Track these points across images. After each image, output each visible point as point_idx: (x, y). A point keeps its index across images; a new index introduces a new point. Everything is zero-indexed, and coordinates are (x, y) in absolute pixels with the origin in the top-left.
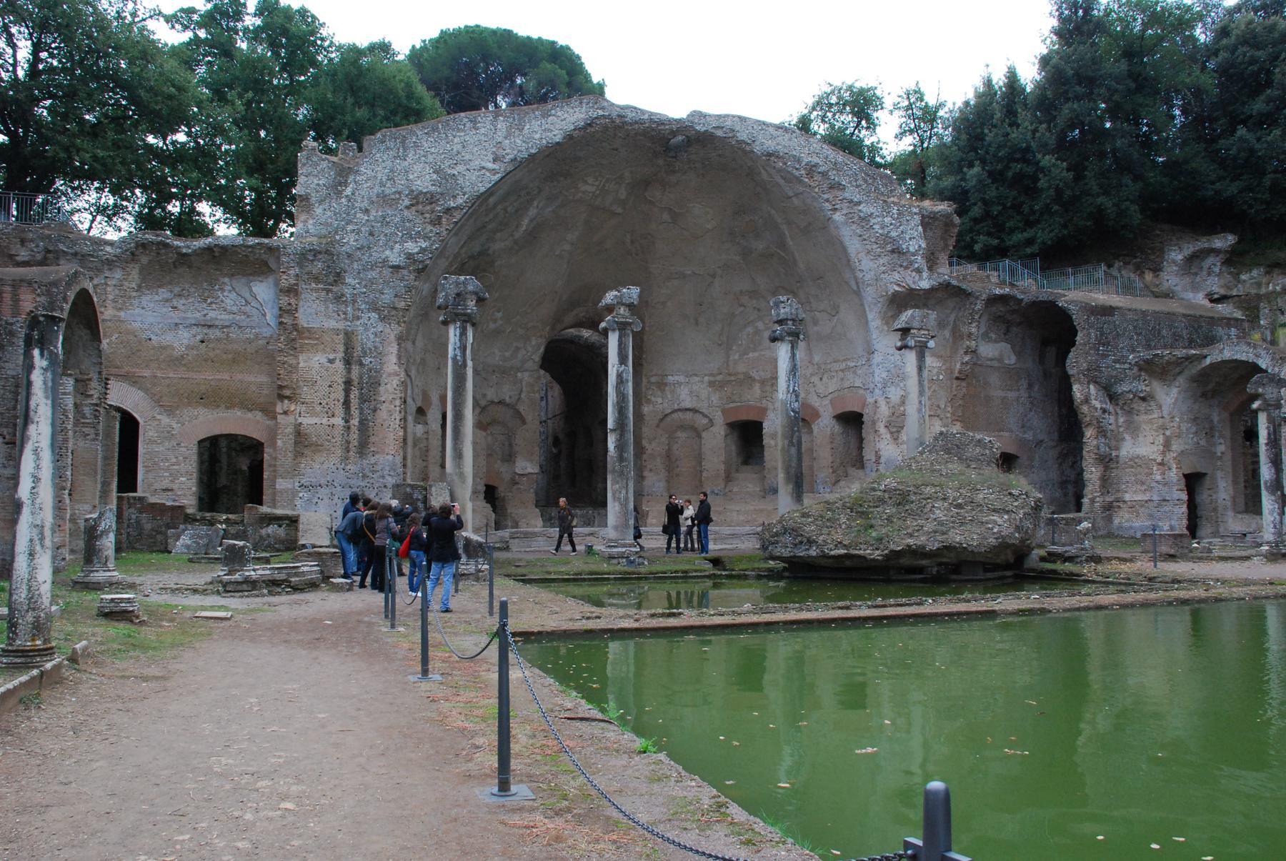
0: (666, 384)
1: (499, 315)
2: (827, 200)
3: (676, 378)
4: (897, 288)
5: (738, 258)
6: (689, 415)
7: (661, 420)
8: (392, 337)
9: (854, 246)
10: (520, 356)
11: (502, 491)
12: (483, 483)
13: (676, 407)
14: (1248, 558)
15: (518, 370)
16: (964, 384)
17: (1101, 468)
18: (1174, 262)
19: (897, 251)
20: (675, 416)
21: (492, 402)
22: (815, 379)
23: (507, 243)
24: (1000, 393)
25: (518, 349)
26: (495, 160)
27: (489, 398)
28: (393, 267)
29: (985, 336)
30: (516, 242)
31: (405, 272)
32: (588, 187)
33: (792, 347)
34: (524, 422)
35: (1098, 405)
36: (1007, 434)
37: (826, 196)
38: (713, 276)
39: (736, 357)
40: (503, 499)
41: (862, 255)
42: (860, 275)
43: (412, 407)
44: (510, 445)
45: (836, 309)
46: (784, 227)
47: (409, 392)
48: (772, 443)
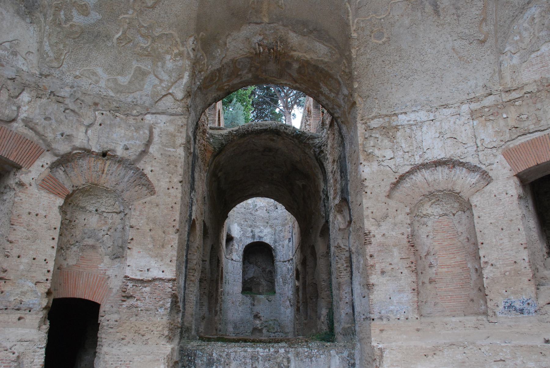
0: (396, 128)
3: (412, 116)
10: (148, 88)
13: (418, 160)
20: (418, 177)
39: (516, 60)
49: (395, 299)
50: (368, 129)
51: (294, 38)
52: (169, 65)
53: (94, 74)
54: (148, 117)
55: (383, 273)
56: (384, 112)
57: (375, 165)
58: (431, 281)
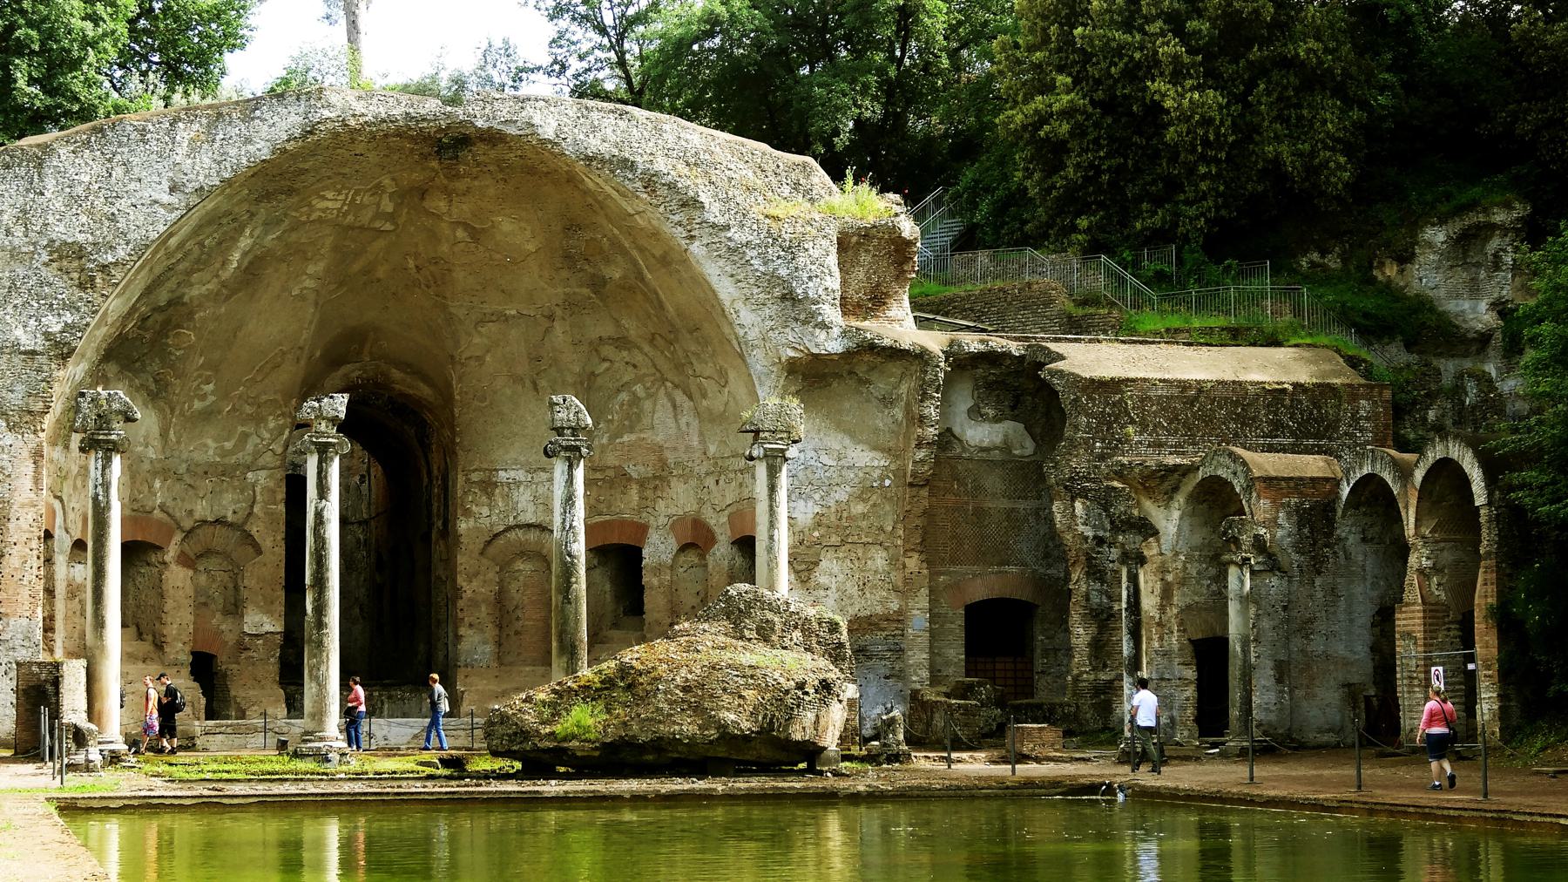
0: (495, 485)
1: (211, 387)
2: (680, 224)
3: (512, 474)
4: (792, 353)
5: (586, 291)
6: (533, 536)
7: (489, 543)
8: (26, 454)
9: (726, 290)
10: (250, 447)
11: (224, 662)
12: (188, 649)
13: (511, 521)
14: (1089, 760)
15: (249, 468)
16: (924, 492)
17: (1093, 630)
18: (1430, 245)
19: (789, 297)
20: (512, 535)
21: (205, 522)
22: (710, 481)
23: (209, 286)
24: (1005, 504)
25: (246, 436)
26: (172, 190)
27: (197, 516)
28: (25, 353)
29: (975, 413)
30: (224, 285)
31: (43, 359)
32: (330, 203)
33: (571, 467)
34: (258, 551)
35: (1090, 534)
36: (1013, 569)
37: (677, 218)
38: (551, 318)
39: (605, 441)
40: (225, 675)
41: (739, 305)
42: (741, 332)
43: (63, 542)
44: (236, 588)
45: (722, 373)
46: (635, 253)
47: (59, 520)
48: (655, 581)
49: (479, 650)
50: (468, 481)
51: (396, 374)
52: (272, 425)
53: (205, 445)
54: (250, 475)
55: (471, 625)
56: (485, 466)
57: (471, 522)
58: (517, 633)
